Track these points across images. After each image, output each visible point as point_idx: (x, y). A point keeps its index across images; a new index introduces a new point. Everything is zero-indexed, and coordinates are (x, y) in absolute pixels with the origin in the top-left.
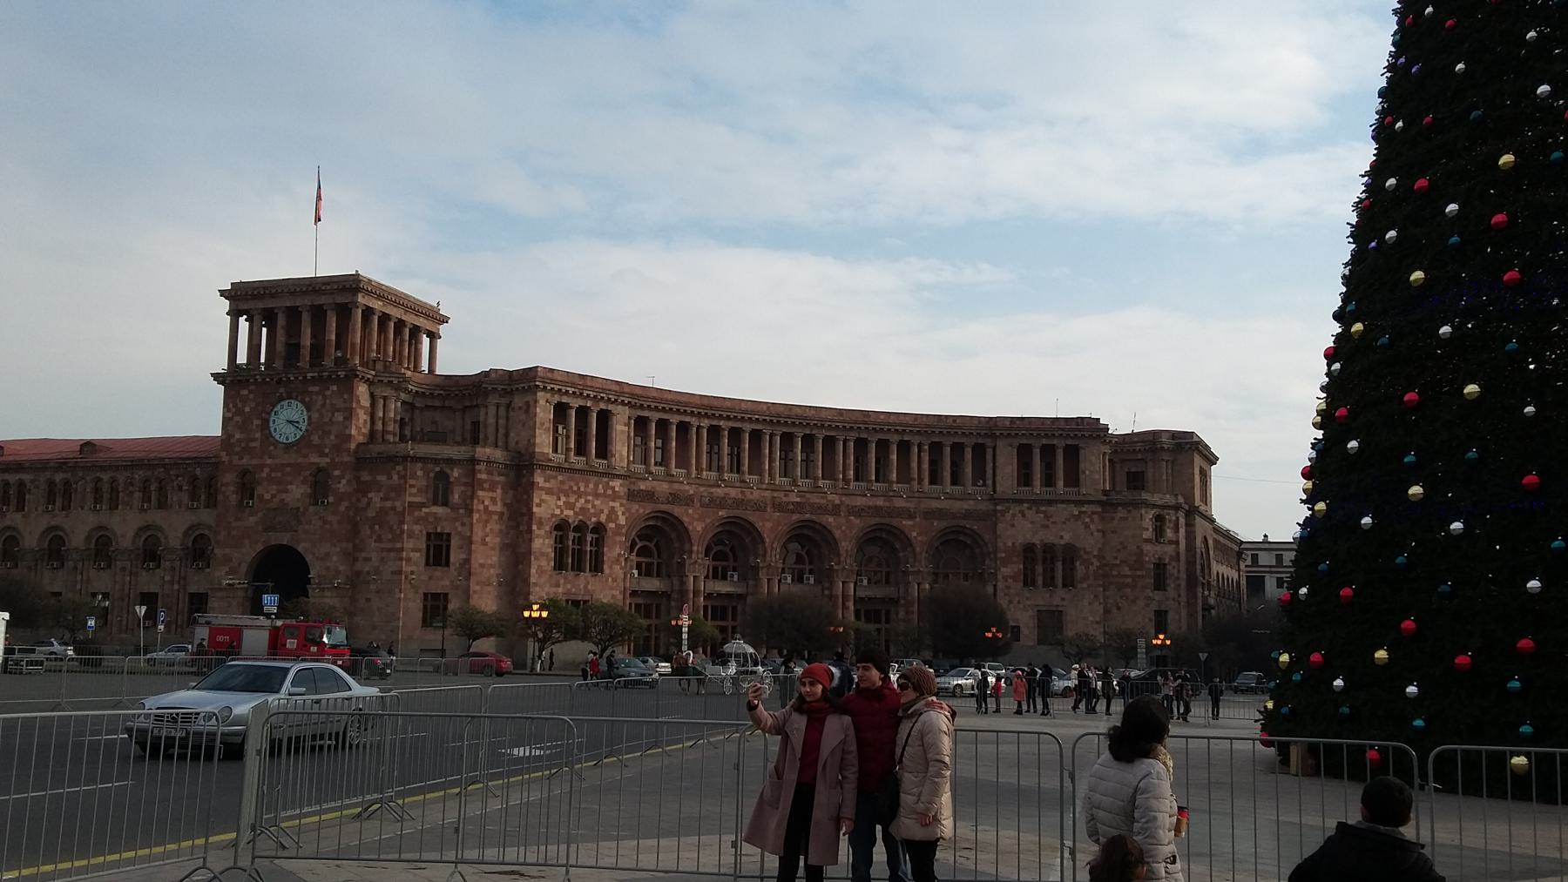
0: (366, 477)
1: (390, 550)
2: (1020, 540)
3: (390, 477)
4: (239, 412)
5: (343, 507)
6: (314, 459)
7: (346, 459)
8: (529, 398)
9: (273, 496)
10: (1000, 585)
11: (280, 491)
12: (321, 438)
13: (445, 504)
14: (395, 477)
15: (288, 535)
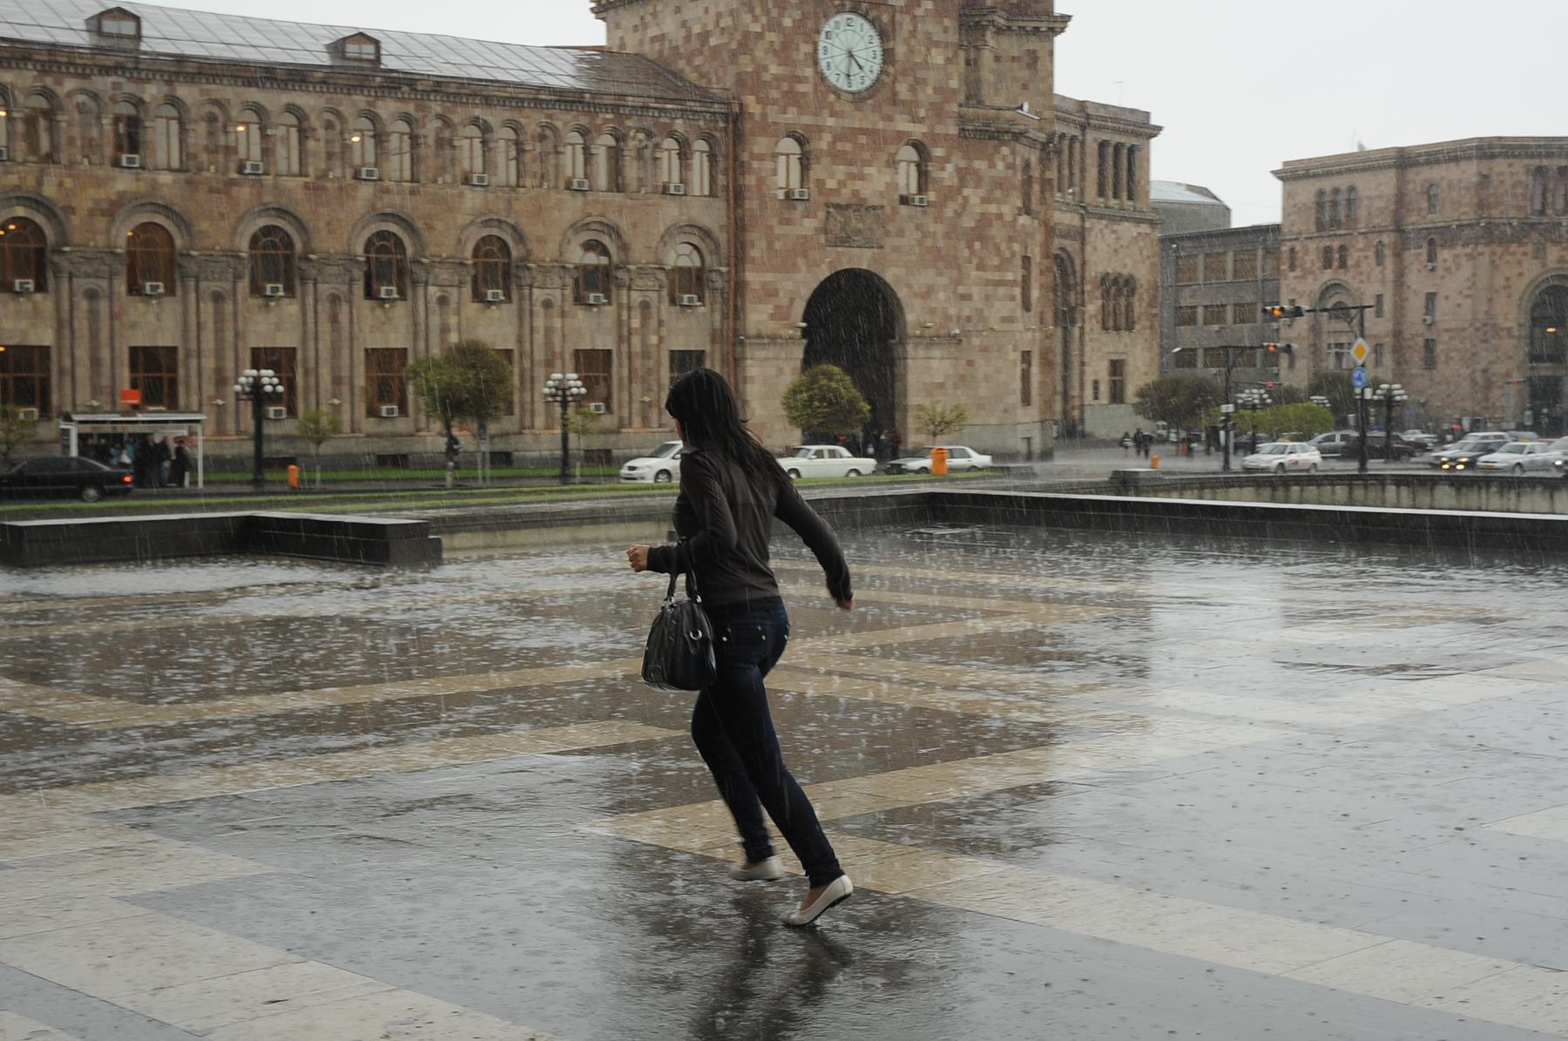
0: (958, 160)
1: (1000, 283)
2: (1101, 269)
3: (993, 166)
4: (774, 25)
5: (949, 212)
6: (903, 124)
7: (953, 130)
8: (1034, 44)
9: (842, 184)
10: (1087, 329)
11: (853, 177)
12: (913, 89)
13: (1027, 210)
14: (1000, 165)
15: (868, 253)
